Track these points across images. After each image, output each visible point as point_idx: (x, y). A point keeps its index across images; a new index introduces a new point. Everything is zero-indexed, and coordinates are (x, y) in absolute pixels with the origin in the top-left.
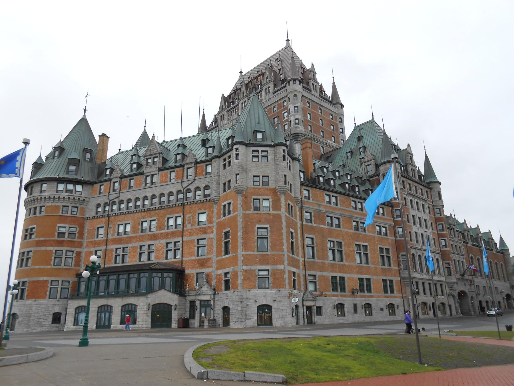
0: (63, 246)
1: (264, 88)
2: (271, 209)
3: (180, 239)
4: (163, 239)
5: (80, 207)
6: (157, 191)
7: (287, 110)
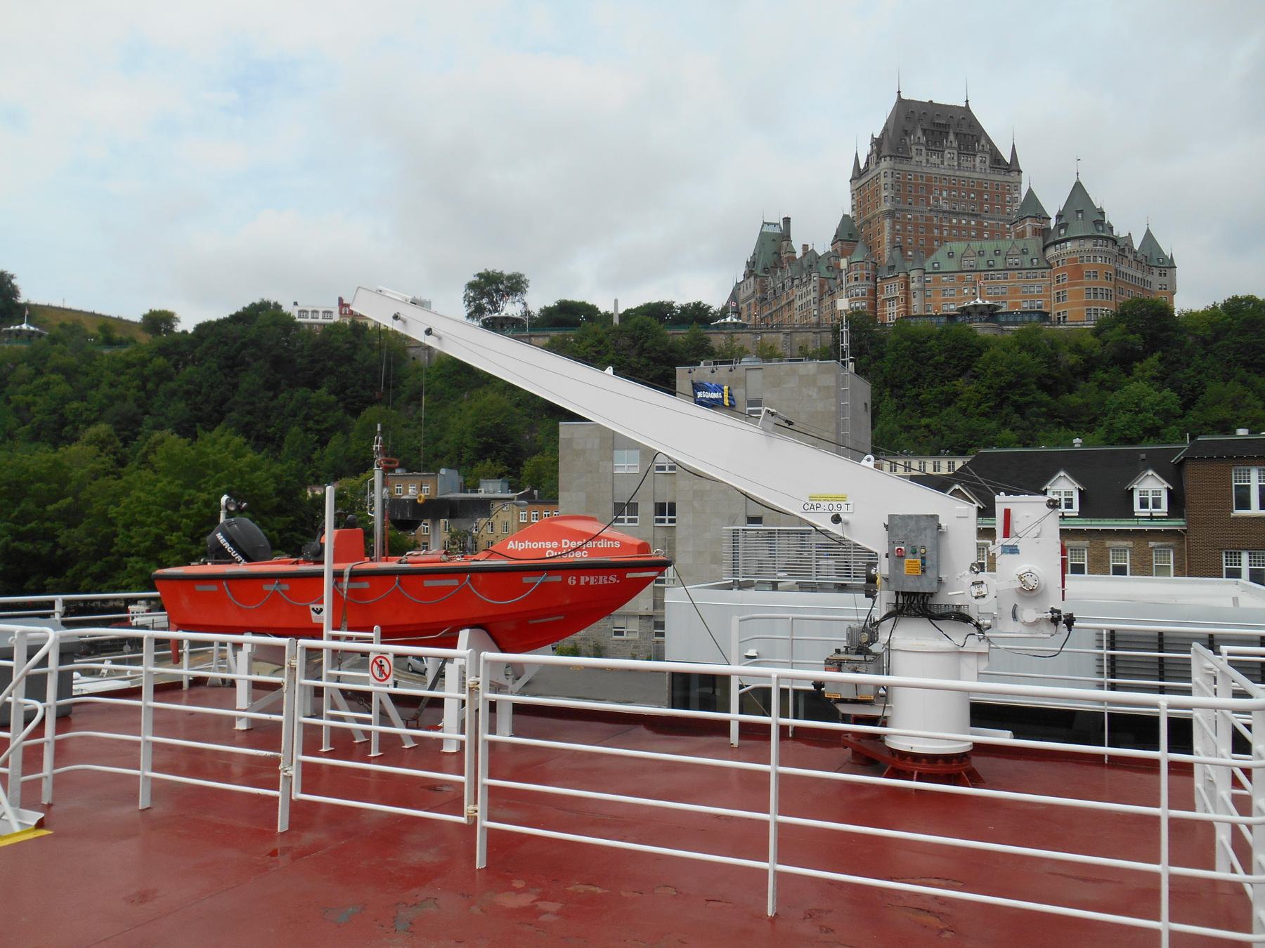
1: (979, 155)
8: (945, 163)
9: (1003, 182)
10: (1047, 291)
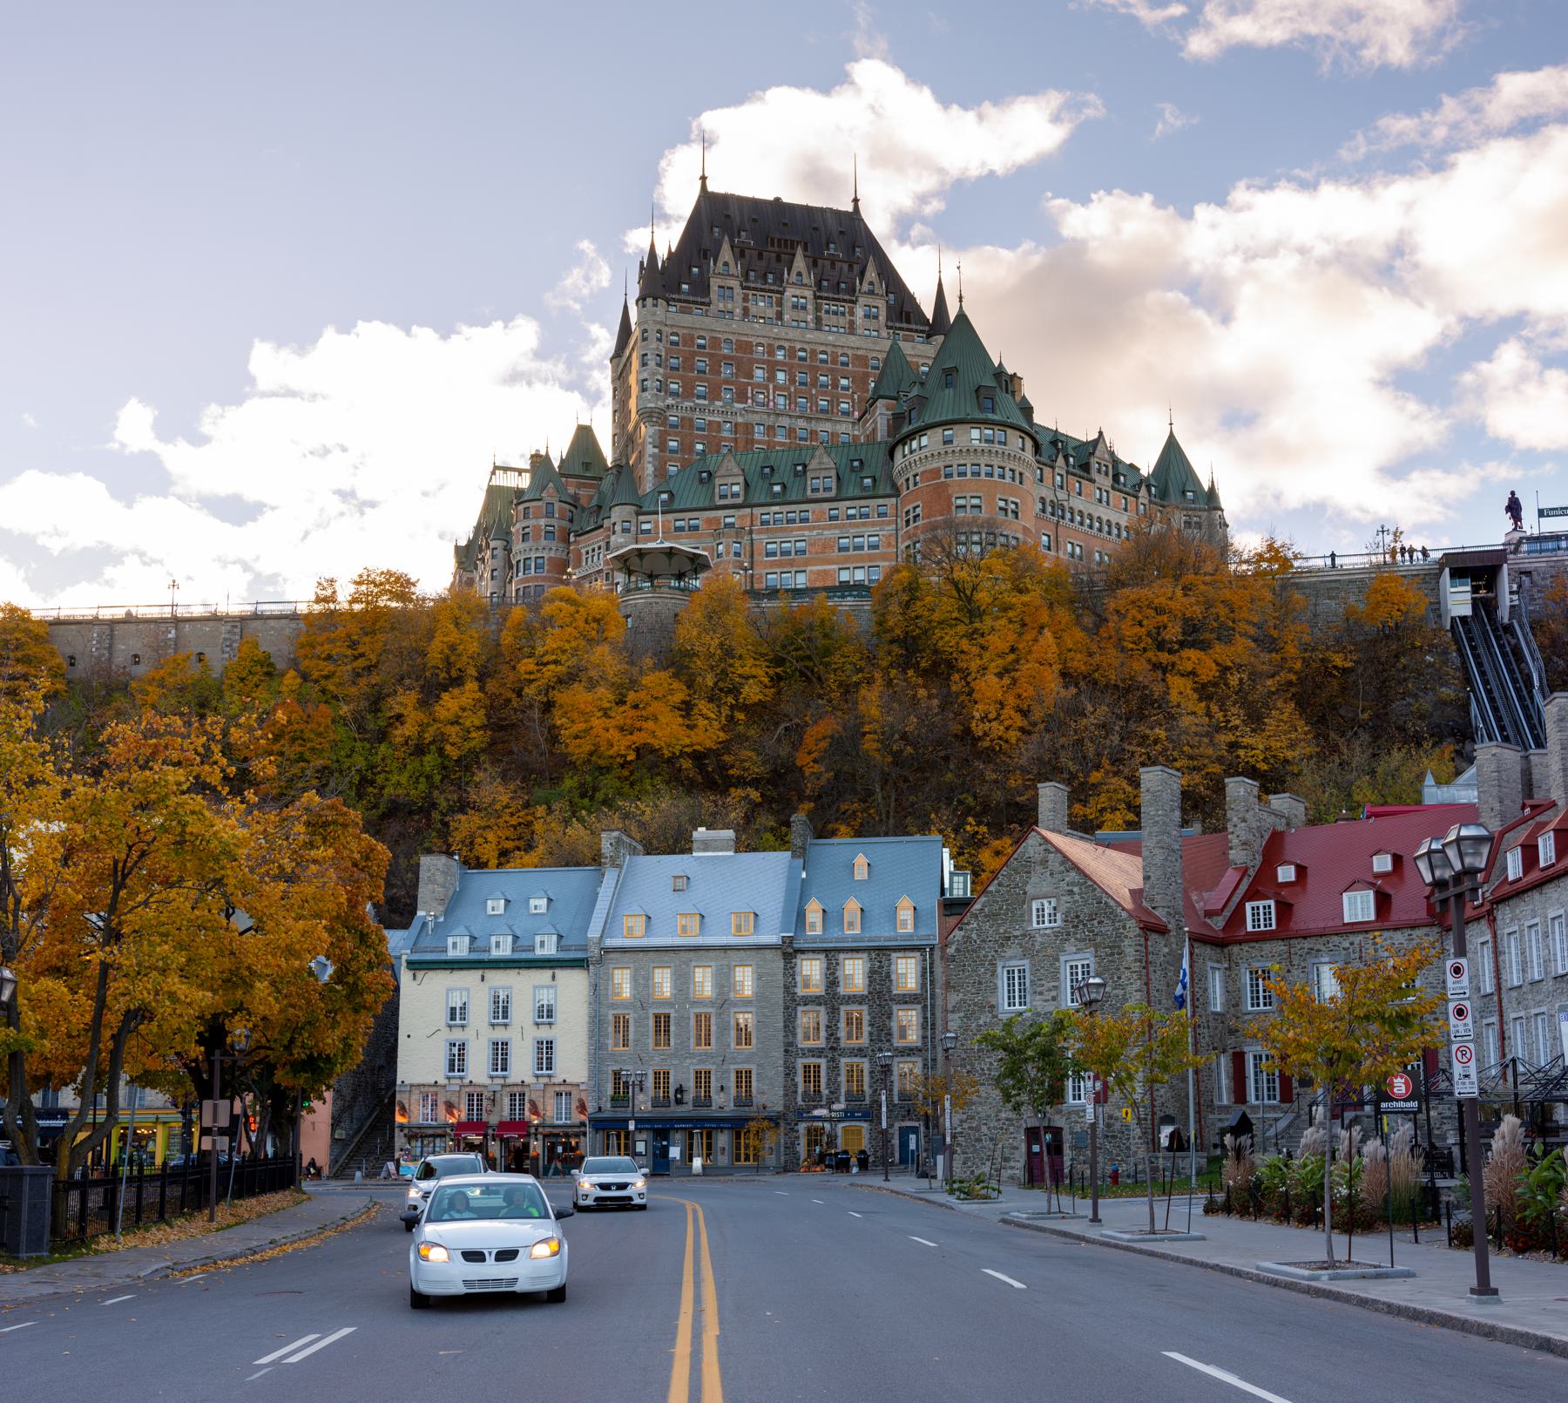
8: (786, 317)
10: (889, 545)
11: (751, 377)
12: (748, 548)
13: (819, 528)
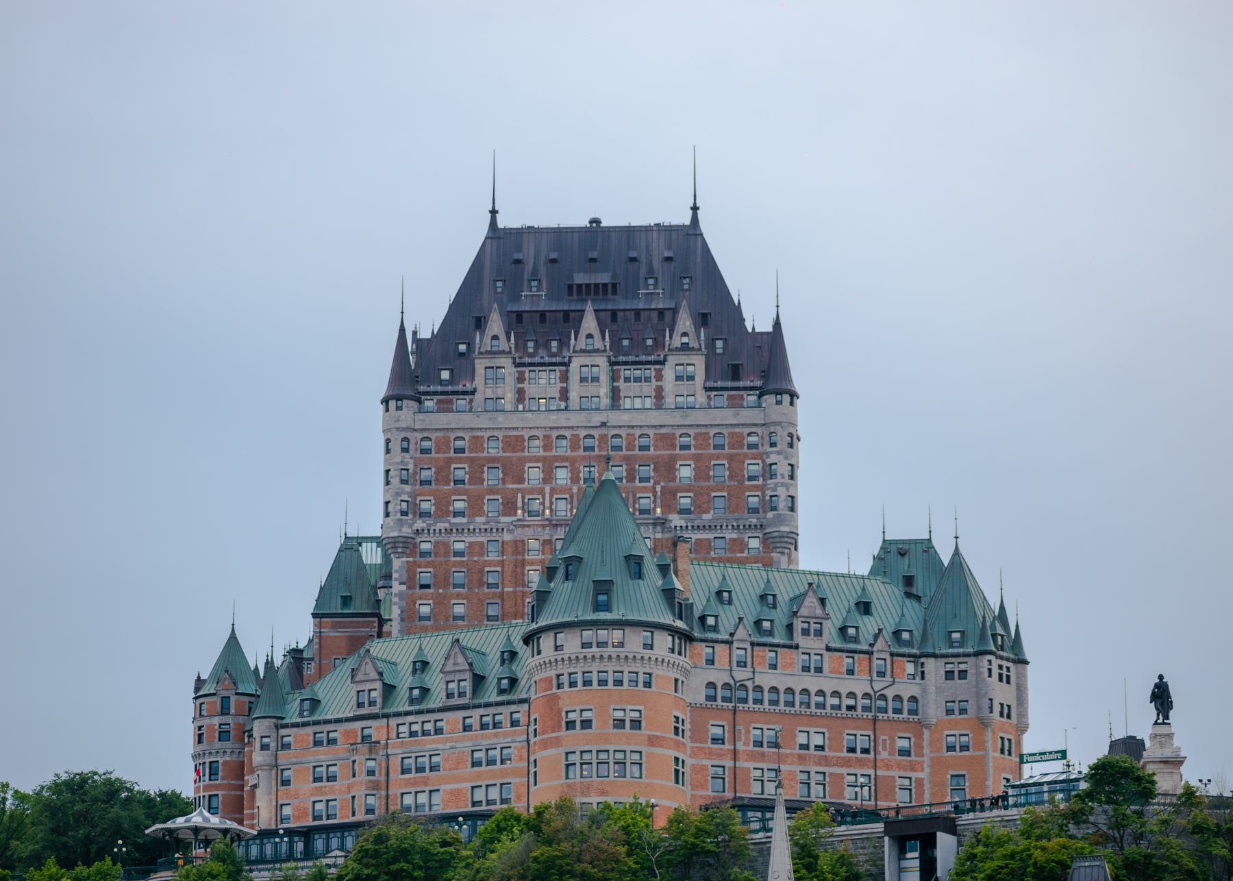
0: (679, 751)
1: (672, 360)
2: (1013, 754)
3: (871, 772)
4: (842, 766)
5: (685, 684)
6: (828, 686)
7: (760, 462)
8: (573, 395)
9: (738, 425)
11: (521, 480)
12: (384, 765)
13: (451, 740)
